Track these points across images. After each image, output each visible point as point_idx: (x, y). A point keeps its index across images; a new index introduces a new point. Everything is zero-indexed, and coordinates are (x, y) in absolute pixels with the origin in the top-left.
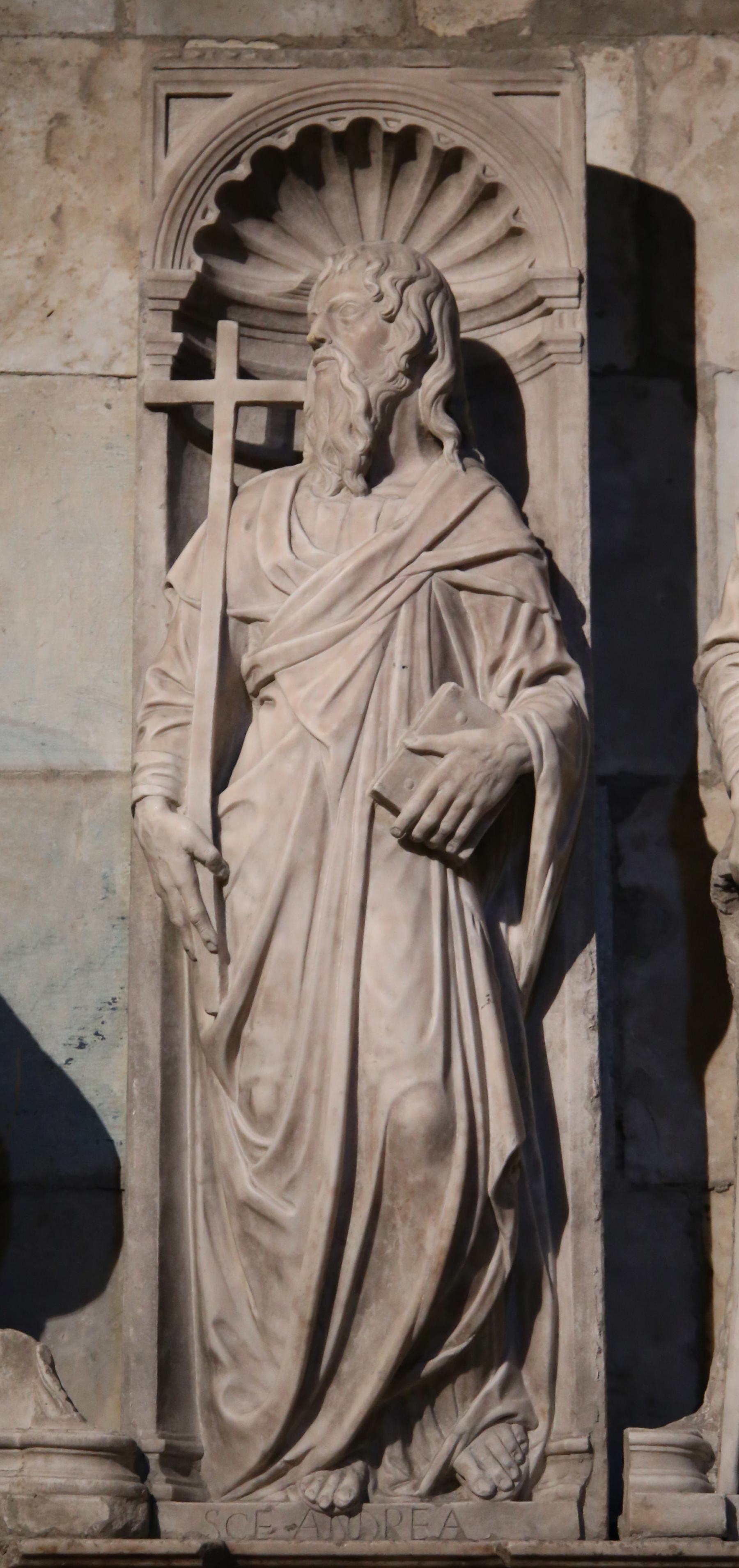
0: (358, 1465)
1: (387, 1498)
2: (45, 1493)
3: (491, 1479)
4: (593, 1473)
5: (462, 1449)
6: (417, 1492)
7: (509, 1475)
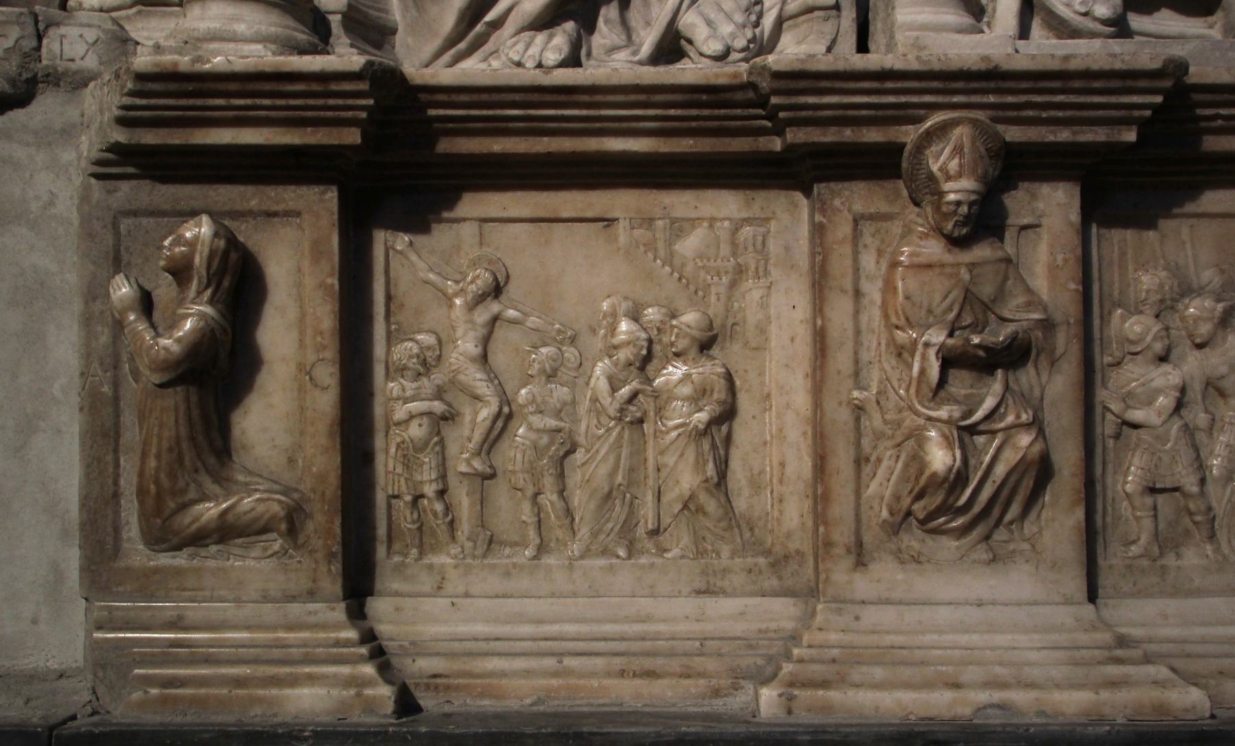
0: (570, 26)
1: (602, 64)
2: (199, 40)
3: (723, 38)
4: (839, 34)
5: (689, 7)
6: (637, 58)
7: (744, 34)
